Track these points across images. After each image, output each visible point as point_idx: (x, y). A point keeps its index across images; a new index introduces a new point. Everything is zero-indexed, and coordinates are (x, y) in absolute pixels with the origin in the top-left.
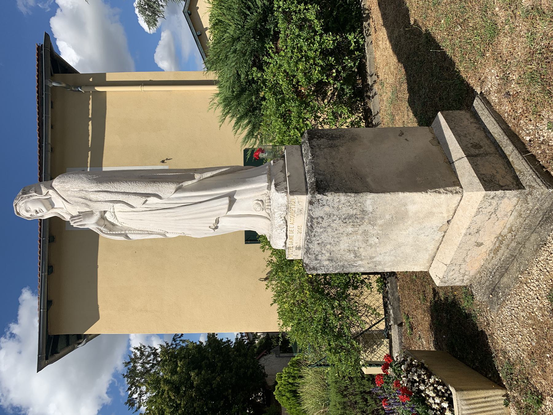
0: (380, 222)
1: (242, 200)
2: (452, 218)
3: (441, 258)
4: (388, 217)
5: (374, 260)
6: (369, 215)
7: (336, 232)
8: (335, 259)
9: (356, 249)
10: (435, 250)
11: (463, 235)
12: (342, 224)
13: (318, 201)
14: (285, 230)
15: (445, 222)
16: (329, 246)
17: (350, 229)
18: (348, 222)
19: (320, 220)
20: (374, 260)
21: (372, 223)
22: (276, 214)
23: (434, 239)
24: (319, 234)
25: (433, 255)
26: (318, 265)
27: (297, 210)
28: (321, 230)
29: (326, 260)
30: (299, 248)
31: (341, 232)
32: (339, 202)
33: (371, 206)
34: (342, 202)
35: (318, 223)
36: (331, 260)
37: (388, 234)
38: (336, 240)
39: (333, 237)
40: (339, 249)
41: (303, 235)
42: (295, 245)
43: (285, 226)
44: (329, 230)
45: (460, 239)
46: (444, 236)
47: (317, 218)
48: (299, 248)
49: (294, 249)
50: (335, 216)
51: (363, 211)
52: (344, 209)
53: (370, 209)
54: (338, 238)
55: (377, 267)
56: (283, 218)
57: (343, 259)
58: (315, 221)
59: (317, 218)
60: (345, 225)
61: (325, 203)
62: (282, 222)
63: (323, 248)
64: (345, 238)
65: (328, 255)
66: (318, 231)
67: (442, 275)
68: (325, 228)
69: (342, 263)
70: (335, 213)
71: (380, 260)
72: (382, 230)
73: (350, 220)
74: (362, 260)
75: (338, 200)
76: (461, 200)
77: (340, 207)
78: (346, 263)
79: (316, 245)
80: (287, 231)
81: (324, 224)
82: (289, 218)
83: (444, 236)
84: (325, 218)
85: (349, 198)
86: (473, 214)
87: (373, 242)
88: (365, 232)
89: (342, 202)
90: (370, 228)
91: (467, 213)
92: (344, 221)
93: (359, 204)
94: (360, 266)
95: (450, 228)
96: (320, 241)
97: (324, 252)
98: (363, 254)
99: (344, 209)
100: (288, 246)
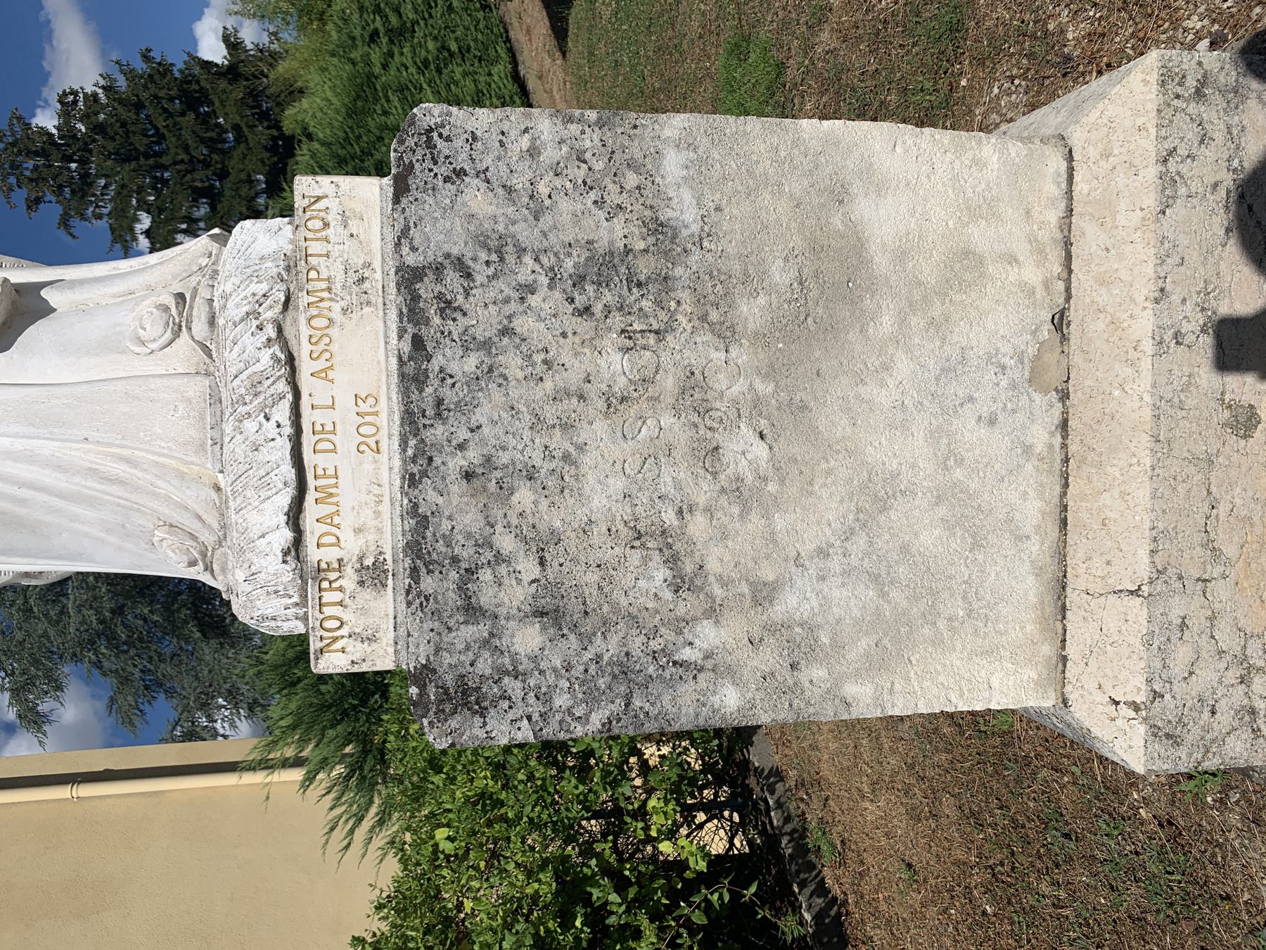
0: (751, 311)
1: (82, 310)
2: (1068, 298)
3: (1098, 565)
4: (780, 275)
5: (778, 611)
6: (695, 257)
7: (548, 385)
8: (574, 607)
9: (670, 517)
10: (1054, 533)
11: (1148, 347)
12: (571, 323)
13: (430, 145)
14: (282, 413)
15: (1046, 331)
16: (524, 496)
17: (614, 365)
18: (598, 308)
19: (453, 279)
20: (778, 611)
21: (714, 316)
22: (230, 304)
23: (1028, 450)
24: (462, 392)
25: (1052, 568)
26: (485, 666)
27: (339, 277)
28: (471, 363)
29: (524, 618)
30: (372, 575)
31: (573, 378)
32: (533, 152)
33: (687, 196)
34: (550, 154)
35: (447, 307)
36: (547, 613)
37: (804, 407)
38: (558, 441)
39: (538, 422)
40: (582, 514)
41: (387, 466)
42: (352, 546)
43: (282, 386)
44: (512, 363)
45: (1146, 382)
46: (1064, 425)
47: (438, 269)
48: (372, 575)
49: (349, 581)
50: (528, 260)
51: (659, 228)
52: (564, 205)
53: (684, 211)
54: (567, 427)
55: (804, 676)
56: (271, 331)
57: (616, 608)
58: (426, 289)
59: (438, 269)
60: (584, 327)
61: (462, 161)
62: (265, 356)
63: (497, 513)
64: (601, 426)
65: (529, 568)
66: (454, 367)
67: (1139, 681)
68: (486, 345)
69: (610, 647)
70: (526, 233)
71: (805, 611)
72: (770, 373)
73: (608, 297)
74: (713, 612)
75: (525, 142)
76: (1071, 170)
77: (543, 189)
78: (636, 644)
79: (457, 488)
80: (298, 431)
81: (482, 317)
82: (305, 331)
83: (1064, 425)
84: (481, 273)
85: (574, 128)
86: (1151, 201)
87: (743, 467)
88: (693, 384)
89: (550, 154)
90: (705, 352)
91: (1121, 219)
92: (580, 300)
93: (631, 180)
94: (713, 666)
95: (1077, 359)
96: (473, 455)
97: (506, 543)
98: (713, 566)
99: (564, 205)
100: (313, 554)
